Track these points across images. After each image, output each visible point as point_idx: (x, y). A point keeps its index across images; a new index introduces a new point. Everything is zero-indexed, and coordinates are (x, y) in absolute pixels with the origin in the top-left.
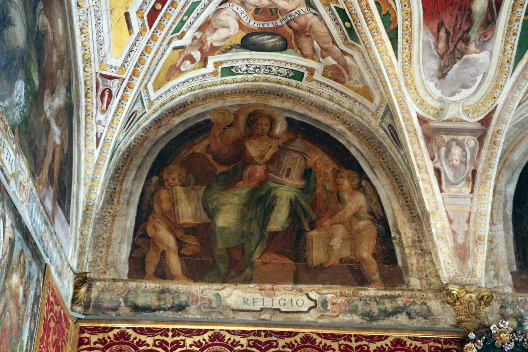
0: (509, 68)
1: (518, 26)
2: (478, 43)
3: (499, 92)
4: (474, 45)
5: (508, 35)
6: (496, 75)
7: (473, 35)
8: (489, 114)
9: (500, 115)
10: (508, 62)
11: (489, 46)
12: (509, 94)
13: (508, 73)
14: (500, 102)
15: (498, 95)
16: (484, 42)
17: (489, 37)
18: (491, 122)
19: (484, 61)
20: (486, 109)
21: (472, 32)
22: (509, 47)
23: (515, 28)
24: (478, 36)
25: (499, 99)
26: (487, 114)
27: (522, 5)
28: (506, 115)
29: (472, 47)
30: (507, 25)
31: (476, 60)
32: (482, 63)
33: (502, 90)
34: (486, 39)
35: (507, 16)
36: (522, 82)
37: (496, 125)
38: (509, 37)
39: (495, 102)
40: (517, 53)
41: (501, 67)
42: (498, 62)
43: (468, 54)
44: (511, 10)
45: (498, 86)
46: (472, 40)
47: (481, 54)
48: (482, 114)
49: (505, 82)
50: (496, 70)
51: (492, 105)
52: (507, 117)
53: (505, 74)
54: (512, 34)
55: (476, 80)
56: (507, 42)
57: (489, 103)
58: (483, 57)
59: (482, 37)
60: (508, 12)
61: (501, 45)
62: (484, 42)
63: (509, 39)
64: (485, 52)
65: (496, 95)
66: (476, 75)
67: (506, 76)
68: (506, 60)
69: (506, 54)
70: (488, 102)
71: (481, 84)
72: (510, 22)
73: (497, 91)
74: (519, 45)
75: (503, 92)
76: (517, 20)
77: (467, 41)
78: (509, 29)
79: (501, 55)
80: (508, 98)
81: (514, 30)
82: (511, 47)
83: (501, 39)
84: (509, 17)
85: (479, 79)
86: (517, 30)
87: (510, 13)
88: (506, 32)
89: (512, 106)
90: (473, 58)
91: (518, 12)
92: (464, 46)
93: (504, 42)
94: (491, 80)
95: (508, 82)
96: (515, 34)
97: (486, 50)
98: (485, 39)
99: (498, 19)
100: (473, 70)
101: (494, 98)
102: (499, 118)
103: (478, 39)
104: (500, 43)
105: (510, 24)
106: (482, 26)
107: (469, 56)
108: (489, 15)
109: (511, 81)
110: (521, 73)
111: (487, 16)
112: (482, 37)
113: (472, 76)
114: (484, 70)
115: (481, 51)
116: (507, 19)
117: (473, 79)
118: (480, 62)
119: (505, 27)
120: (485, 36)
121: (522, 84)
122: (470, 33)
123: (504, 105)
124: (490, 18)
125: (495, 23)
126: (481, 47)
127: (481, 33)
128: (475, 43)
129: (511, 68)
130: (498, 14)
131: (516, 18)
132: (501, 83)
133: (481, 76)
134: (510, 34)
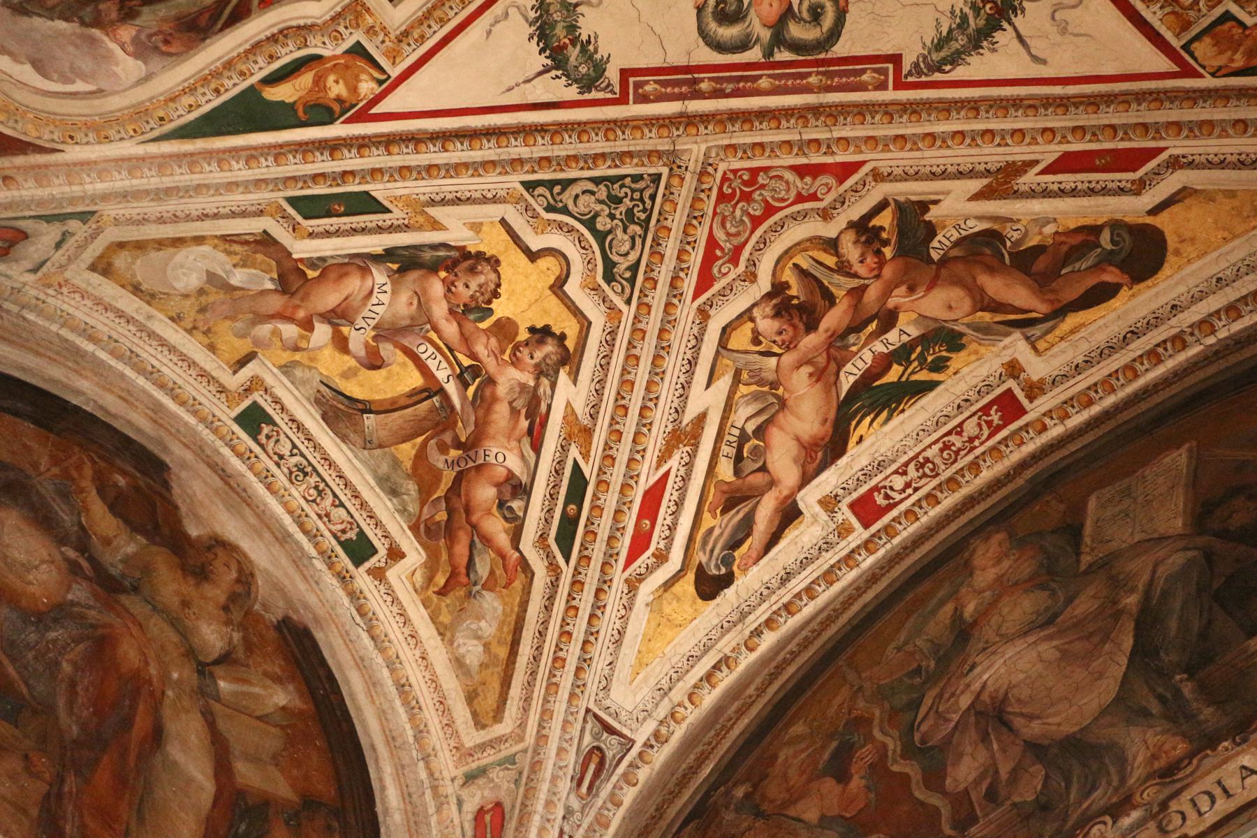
0: (152, 129)
1: (235, 85)
2: (143, 37)
3: (91, 139)
4: (134, 33)
5: (205, 80)
6: (118, 114)
7: (149, 18)
8: (29, 144)
9: (46, 166)
10: (162, 119)
11: (156, 63)
12: (105, 161)
13: (143, 133)
14: (74, 153)
15: (84, 140)
16: (156, 48)
17: (172, 50)
18: (14, 154)
19: (122, 75)
20: (35, 134)
21: (154, 12)
22: (187, 100)
23: (228, 83)
24: (155, 30)
25: (77, 148)
26: (23, 138)
27: (271, 57)
28: (58, 177)
29: (126, 33)
30: (218, 64)
31: (108, 57)
32: (115, 74)
33: (100, 143)
34: (164, 48)
35: (232, 50)
36: (150, 170)
37: (18, 168)
38: (202, 86)
39: (63, 142)
40: (191, 123)
41: (140, 113)
42: (143, 102)
43: (108, 35)
44: (247, 46)
45: (101, 130)
46: (137, 23)
47: (130, 61)
48: (14, 129)
49: (122, 139)
50: (127, 108)
51: (53, 141)
52: (56, 181)
53: (135, 131)
54: (213, 86)
55: (73, 82)
56: (192, 90)
57: (52, 132)
58: (128, 67)
59: (161, 37)
60: (240, 45)
61: (178, 85)
62: (156, 48)
63: (201, 90)
64: (139, 63)
65: (79, 136)
66: (84, 77)
67: (132, 133)
68: (161, 114)
69: (171, 104)
70: (51, 128)
71: (74, 95)
72: (229, 65)
73: (91, 135)
74: (207, 117)
75: (97, 147)
76: (242, 74)
77: (128, 14)
78: (216, 74)
79: (162, 98)
80: (95, 162)
81: (222, 85)
82: (191, 106)
83: (188, 75)
84: (235, 54)
85: (80, 86)
86: (226, 90)
87: (241, 50)
88: (207, 72)
89: (88, 180)
90: (109, 50)
91: (256, 62)
92: (114, 15)
93: (186, 84)
94: (103, 110)
95: (126, 144)
96: (217, 91)
97: (145, 63)
98: (160, 45)
99: (214, 38)
100: (86, 64)
101: (71, 137)
102: (40, 167)
103: (149, 31)
104: (179, 79)
105: (224, 68)
106: (178, 19)
107: (106, 39)
108: (207, 15)
109: (130, 148)
110: (163, 156)
111: (201, 13)
112: (161, 37)
113: (72, 69)
114: (103, 85)
115: (136, 55)
116: (228, 53)
117: (70, 75)
118: (114, 68)
119: (213, 63)
120: (166, 42)
121: (146, 170)
122: (145, 9)
123: (75, 164)
124: (203, 21)
125: (204, 40)
126: (141, 50)
127: (166, 28)
128: (139, 32)
129: (156, 133)
130: (221, 30)
131: (243, 68)
132: (112, 133)
133: (91, 88)
134: (210, 82)
